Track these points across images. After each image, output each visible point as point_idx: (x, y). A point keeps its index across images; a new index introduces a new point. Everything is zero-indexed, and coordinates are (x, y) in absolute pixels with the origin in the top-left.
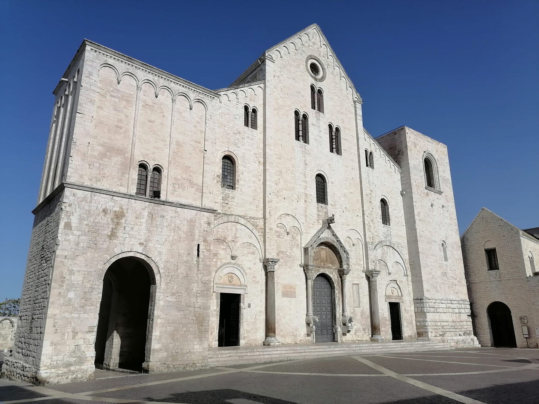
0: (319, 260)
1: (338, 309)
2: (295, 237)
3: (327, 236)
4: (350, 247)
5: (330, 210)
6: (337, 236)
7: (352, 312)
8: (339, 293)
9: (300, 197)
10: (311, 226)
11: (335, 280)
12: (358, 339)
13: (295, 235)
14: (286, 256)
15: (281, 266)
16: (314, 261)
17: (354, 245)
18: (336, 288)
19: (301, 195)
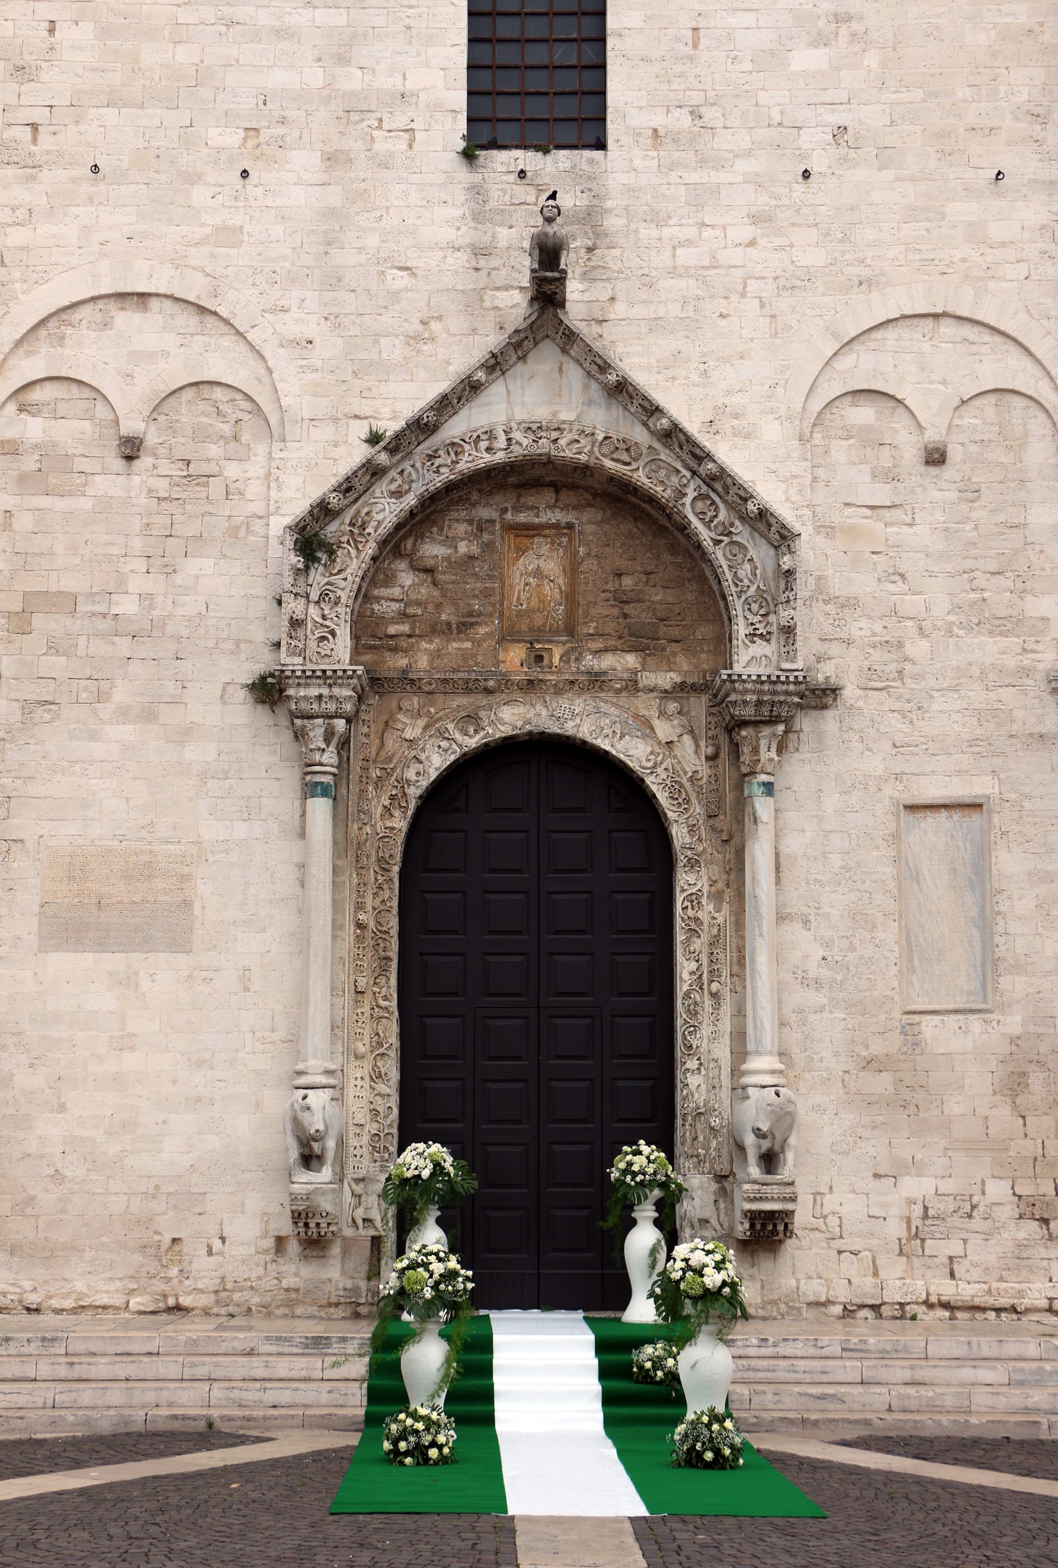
0: (482, 630)
1: (706, 1030)
2: (212, 468)
3: (541, 413)
4: (891, 477)
5: (632, 191)
6: (645, 398)
7: (877, 1047)
8: (717, 897)
9: (281, 130)
10: (393, 350)
11: (676, 789)
12: (947, 1290)
13: (214, 450)
14: (103, 625)
15: (40, 714)
16: (424, 645)
17: (936, 458)
18: (681, 860)
19: (283, 121)
